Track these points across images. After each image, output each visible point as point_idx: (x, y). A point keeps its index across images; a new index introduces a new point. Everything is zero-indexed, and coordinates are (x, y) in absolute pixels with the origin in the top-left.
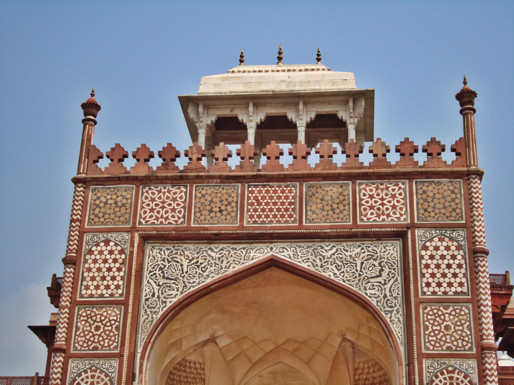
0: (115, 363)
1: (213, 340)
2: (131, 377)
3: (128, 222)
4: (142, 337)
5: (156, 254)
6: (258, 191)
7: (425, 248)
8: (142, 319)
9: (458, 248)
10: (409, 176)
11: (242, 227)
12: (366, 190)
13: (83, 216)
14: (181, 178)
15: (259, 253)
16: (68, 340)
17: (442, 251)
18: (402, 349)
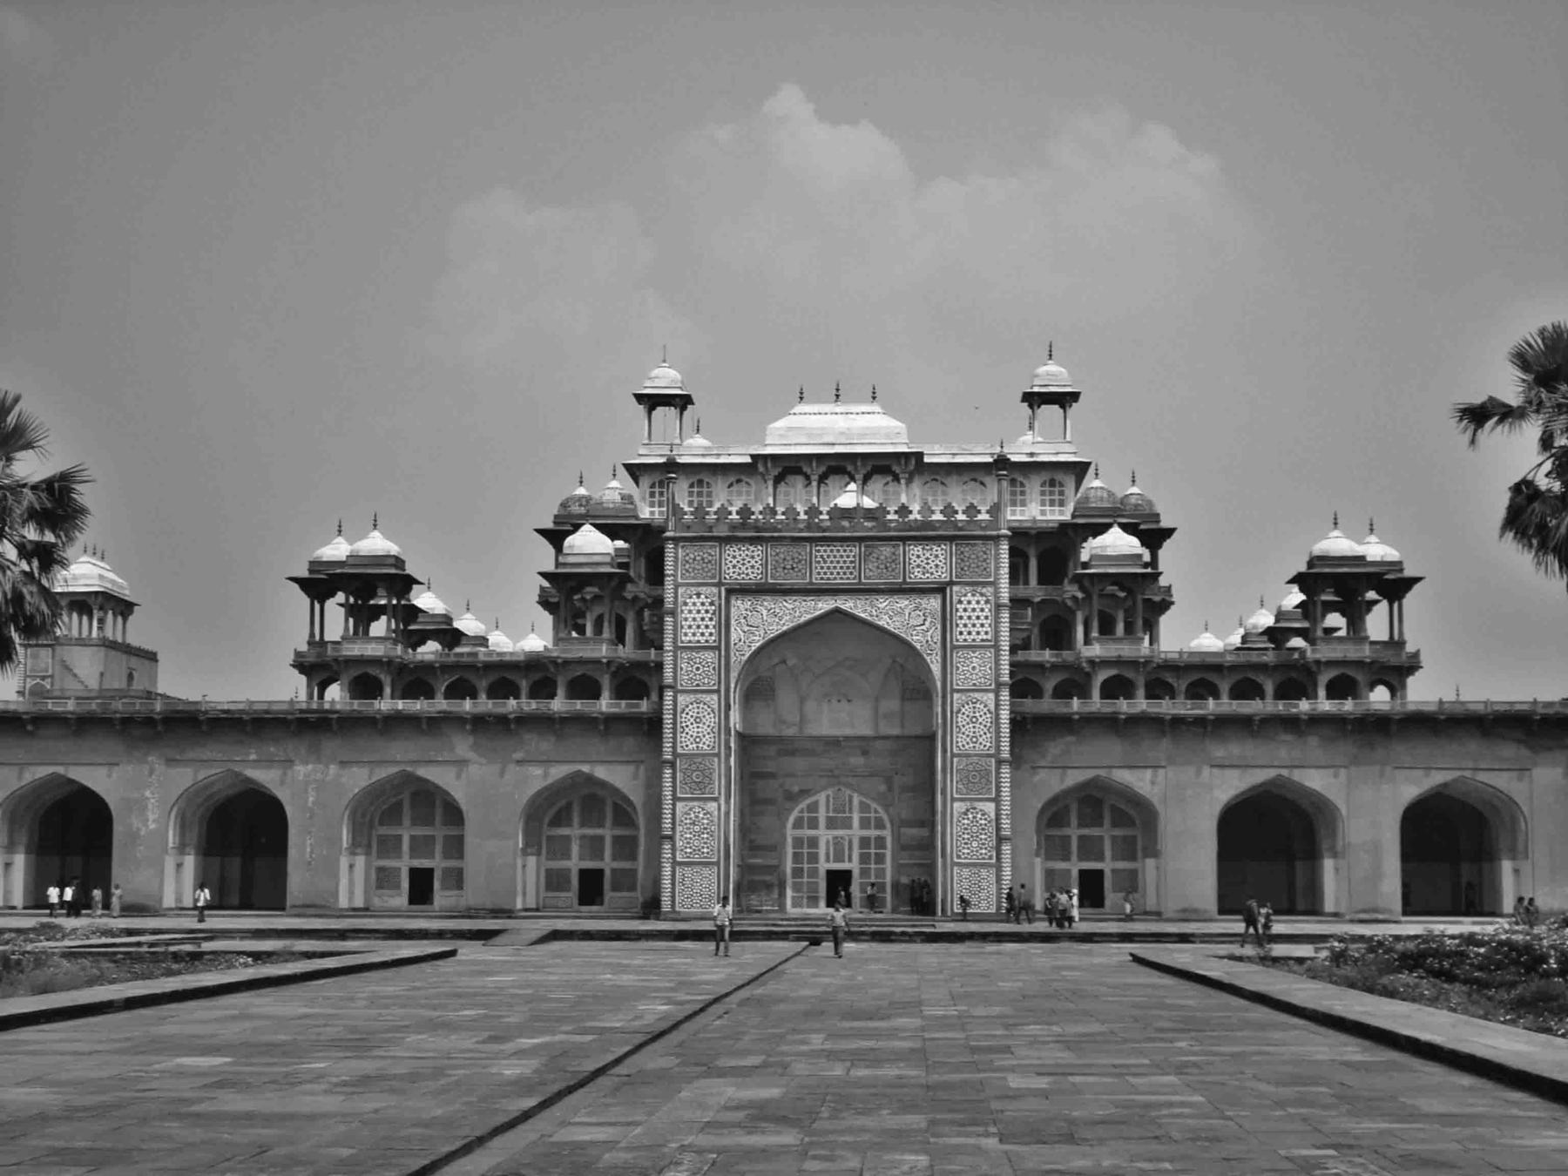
0: (715, 697)
1: (784, 662)
2: (728, 707)
3: (713, 577)
4: (734, 675)
5: (740, 606)
6: (823, 550)
7: (960, 602)
8: (733, 659)
9: (987, 602)
10: (951, 539)
11: (811, 583)
12: (915, 551)
13: (676, 570)
14: (758, 538)
15: (824, 605)
16: (675, 678)
17: (974, 605)
18: (939, 684)
